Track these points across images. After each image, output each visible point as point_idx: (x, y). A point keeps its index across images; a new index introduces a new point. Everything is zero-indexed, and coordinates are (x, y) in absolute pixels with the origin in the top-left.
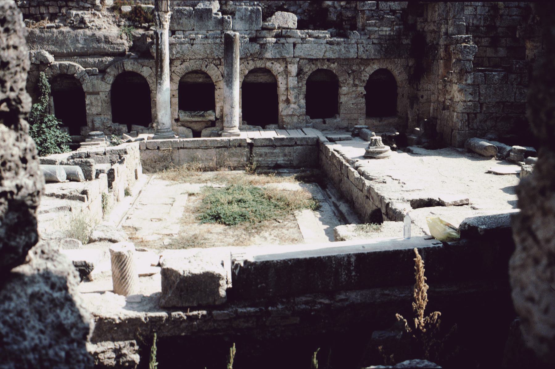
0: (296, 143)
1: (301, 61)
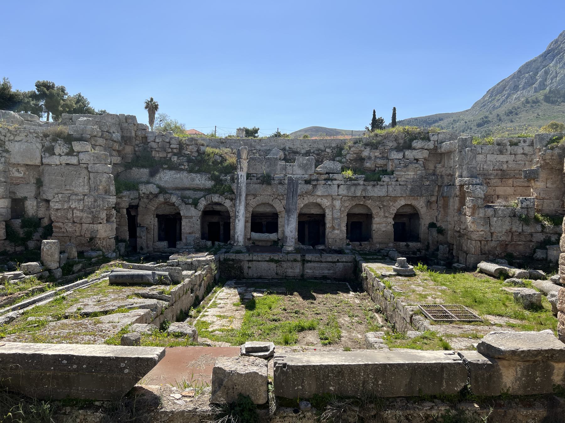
1: (344, 198)
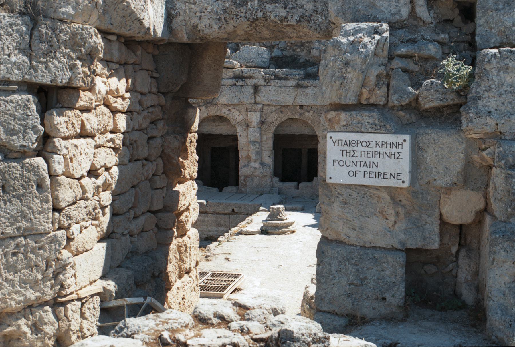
0: (233, 210)
